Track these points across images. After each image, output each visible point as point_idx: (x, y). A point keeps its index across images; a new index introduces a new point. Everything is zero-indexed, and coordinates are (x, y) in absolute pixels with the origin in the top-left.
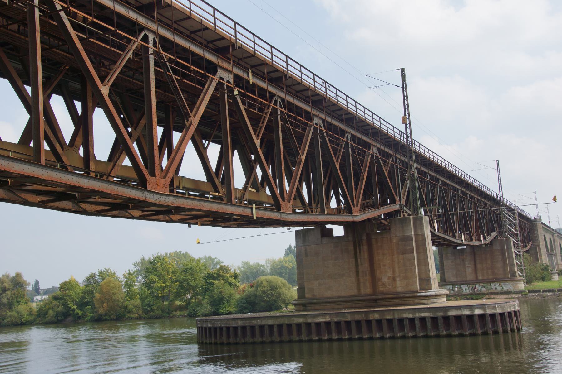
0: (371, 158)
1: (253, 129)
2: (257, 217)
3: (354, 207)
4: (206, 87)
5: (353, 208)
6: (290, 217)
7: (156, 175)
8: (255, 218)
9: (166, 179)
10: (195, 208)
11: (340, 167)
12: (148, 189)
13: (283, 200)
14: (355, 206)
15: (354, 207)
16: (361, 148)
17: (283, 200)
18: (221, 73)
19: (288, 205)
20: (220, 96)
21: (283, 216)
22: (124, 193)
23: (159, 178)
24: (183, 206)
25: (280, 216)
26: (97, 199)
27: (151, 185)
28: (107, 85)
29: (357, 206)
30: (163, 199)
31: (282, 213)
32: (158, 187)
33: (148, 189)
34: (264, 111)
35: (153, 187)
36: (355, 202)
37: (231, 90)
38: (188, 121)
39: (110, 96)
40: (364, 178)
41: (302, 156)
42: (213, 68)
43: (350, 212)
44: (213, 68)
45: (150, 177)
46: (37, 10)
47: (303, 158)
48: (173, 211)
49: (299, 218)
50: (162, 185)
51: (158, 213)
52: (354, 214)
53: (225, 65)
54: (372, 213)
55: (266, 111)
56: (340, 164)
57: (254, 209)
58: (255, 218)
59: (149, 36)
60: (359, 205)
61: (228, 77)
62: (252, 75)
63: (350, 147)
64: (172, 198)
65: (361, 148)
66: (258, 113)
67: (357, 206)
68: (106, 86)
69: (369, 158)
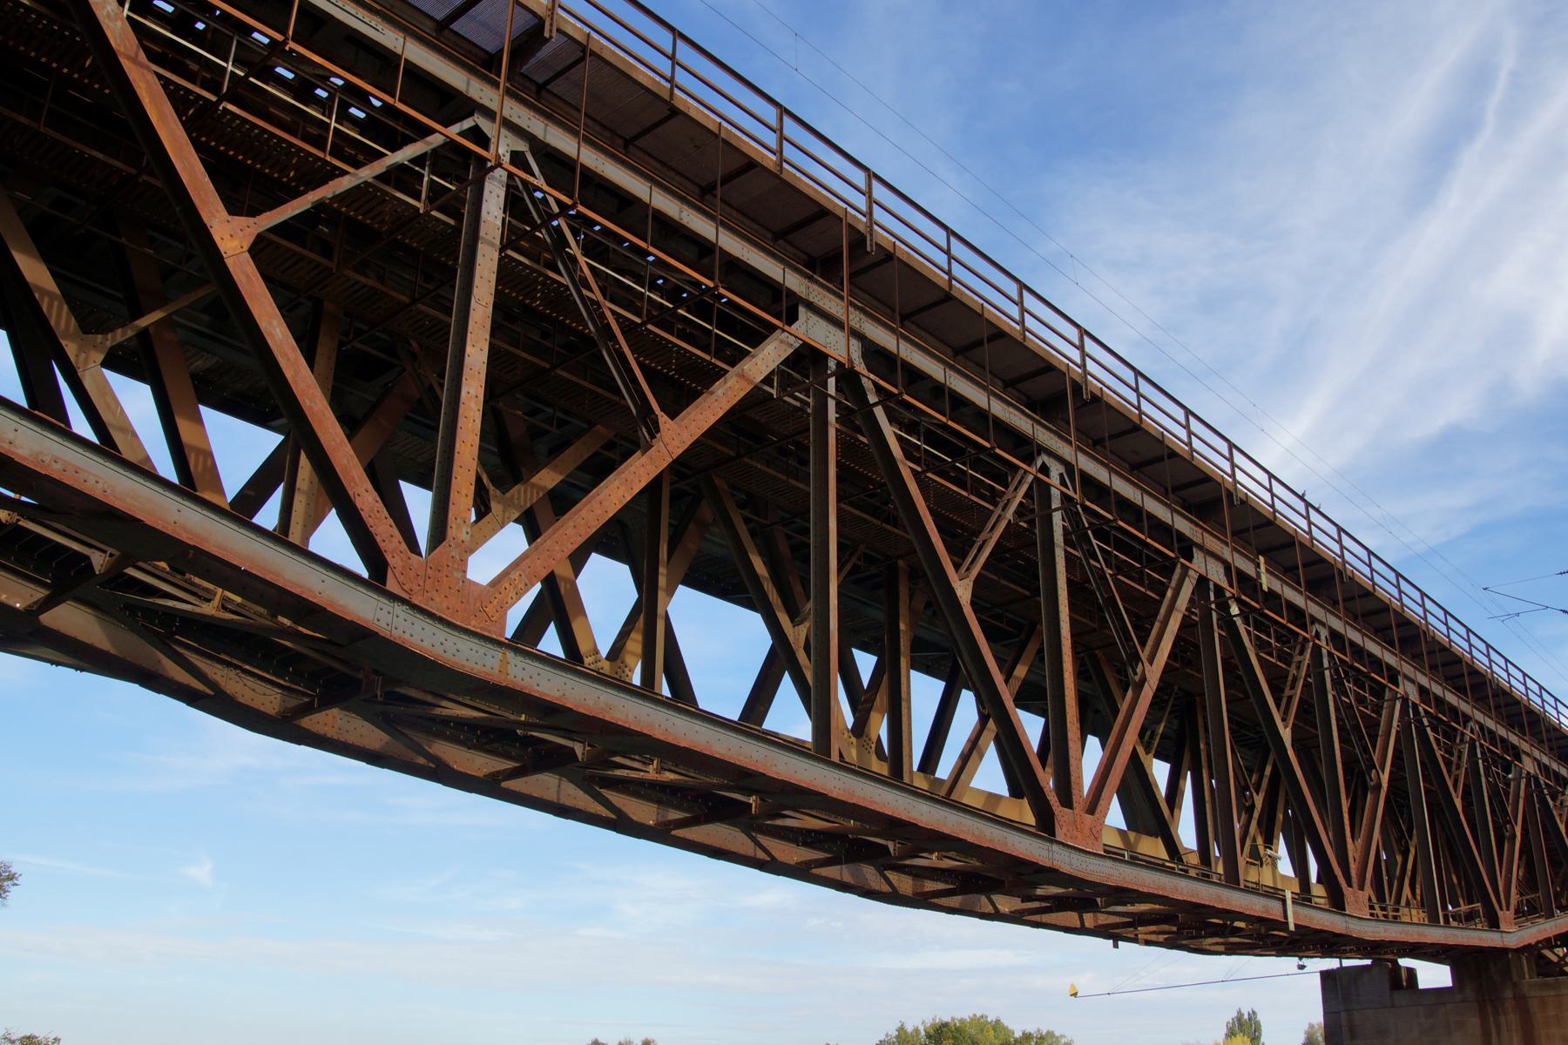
0: (1528, 785)
1: (1276, 703)
2: (1296, 925)
3: (1501, 909)
4: (1169, 593)
5: (1500, 913)
6: (1366, 929)
7: (1075, 805)
8: (1292, 927)
9: (1097, 815)
10: (1161, 893)
11: (1463, 807)
12: (1058, 838)
13: (1350, 885)
14: (1504, 908)
15: (1501, 909)
16: (1508, 758)
17: (1350, 885)
18: (1199, 563)
19: (1361, 896)
20: (1200, 618)
21: (1351, 926)
22: (1006, 845)
23: (1082, 813)
24: (1136, 888)
25: (1344, 925)
26: (932, 860)
27: (1064, 830)
28: (968, 577)
29: (1508, 909)
30: (1091, 867)
31: (1349, 915)
32: (1079, 835)
33: (1058, 839)
34: (1292, 658)
35: (1068, 835)
36: (1502, 897)
37: (1224, 607)
38: (1136, 674)
39: (973, 603)
40: (1514, 836)
41: (1381, 773)
42: (1186, 548)
43: (1494, 924)
44: (1186, 548)
45: (1061, 808)
46: (831, 404)
47: (1385, 778)
48: (1099, 900)
49: (1385, 930)
50: (1087, 831)
51: (1059, 904)
52: (1503, 927)
53: (1212, 543)
54: (1542, 927)
55: (1297, 658)
56: (1462, 799)
57: (1289, 902)
58: (1292, 927)
59: (1051, 469)
60: (1512, 907)
61: (1216, 574)
62: (1267, 570)
63: (1479, 756)
64: (1109, 863)
65: (1508, 758)
66: (1279, 663)
67: (1508, 909)
68: (966, 581)
69: (1523, 786)
